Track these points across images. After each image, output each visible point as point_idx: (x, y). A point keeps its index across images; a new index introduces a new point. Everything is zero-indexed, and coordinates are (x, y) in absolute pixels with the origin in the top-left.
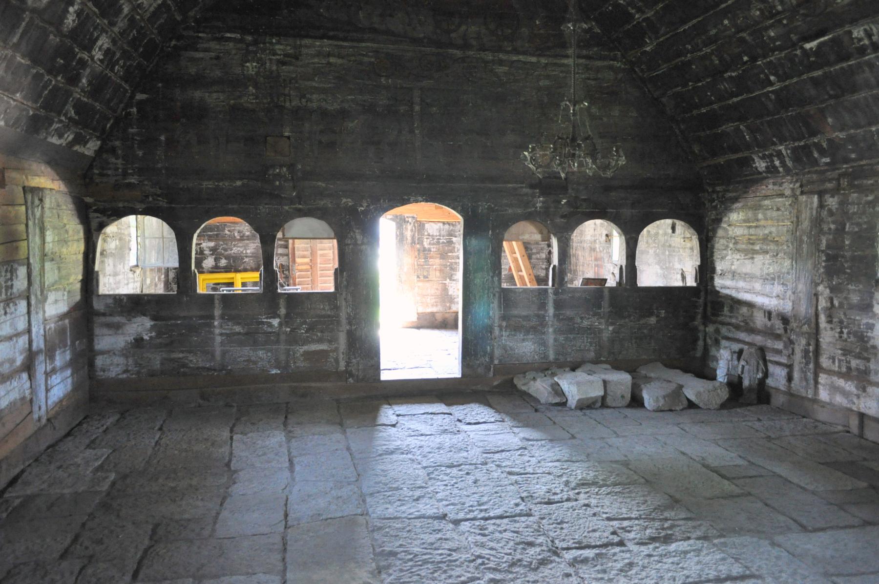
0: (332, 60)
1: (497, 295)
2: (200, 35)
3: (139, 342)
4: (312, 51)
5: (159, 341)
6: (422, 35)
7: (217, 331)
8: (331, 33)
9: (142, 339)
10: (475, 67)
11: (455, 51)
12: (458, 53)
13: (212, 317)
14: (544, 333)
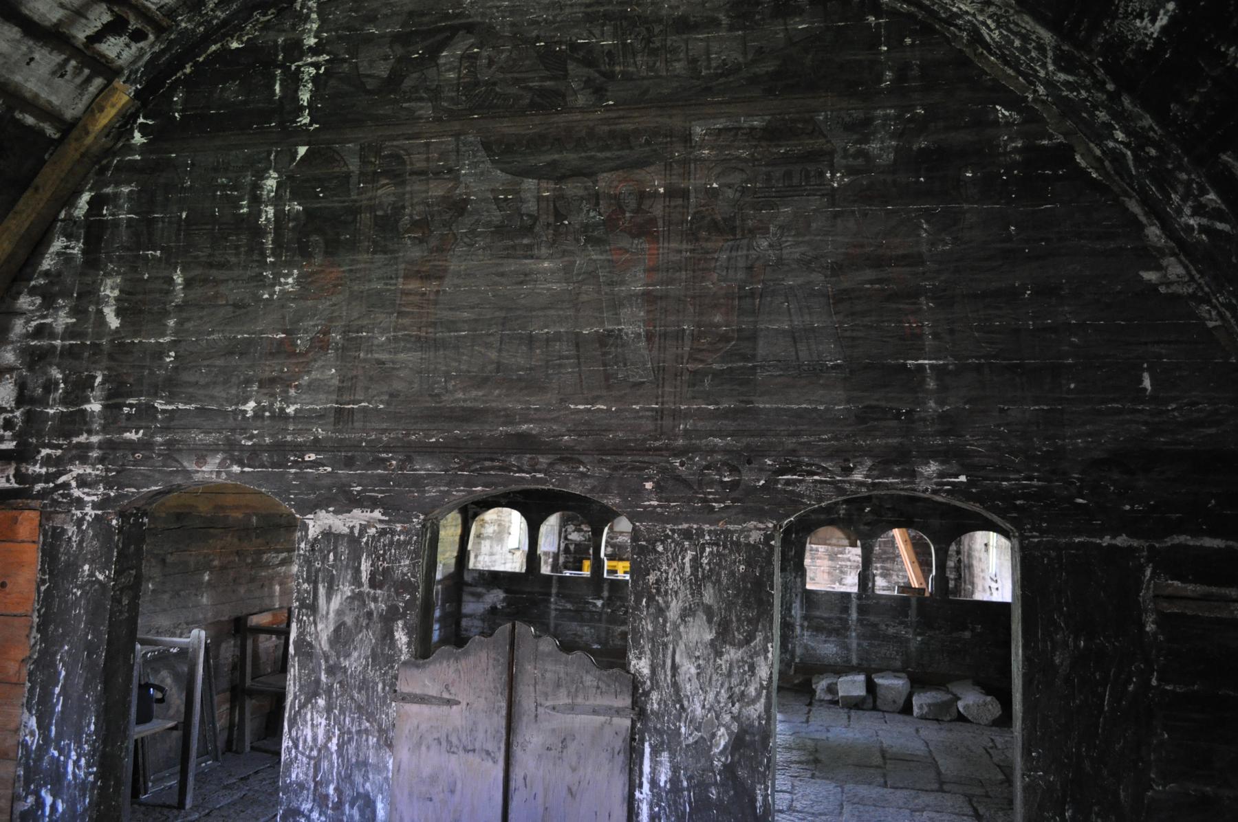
1: (799, 596)
3: (493, 609)
5: (508, 610)
7: (553, 607)
9: (496, 608)
13: (550, 595)
14: (847, 637)
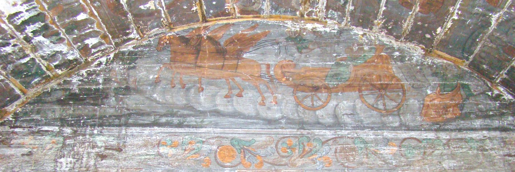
0: (163, 150)
2: (17, 130)
4: (139, 141)
6: (278, 115)
8: (164, 120)
10: (353, 149)
11: (323, 132)
12: (329, 134)
